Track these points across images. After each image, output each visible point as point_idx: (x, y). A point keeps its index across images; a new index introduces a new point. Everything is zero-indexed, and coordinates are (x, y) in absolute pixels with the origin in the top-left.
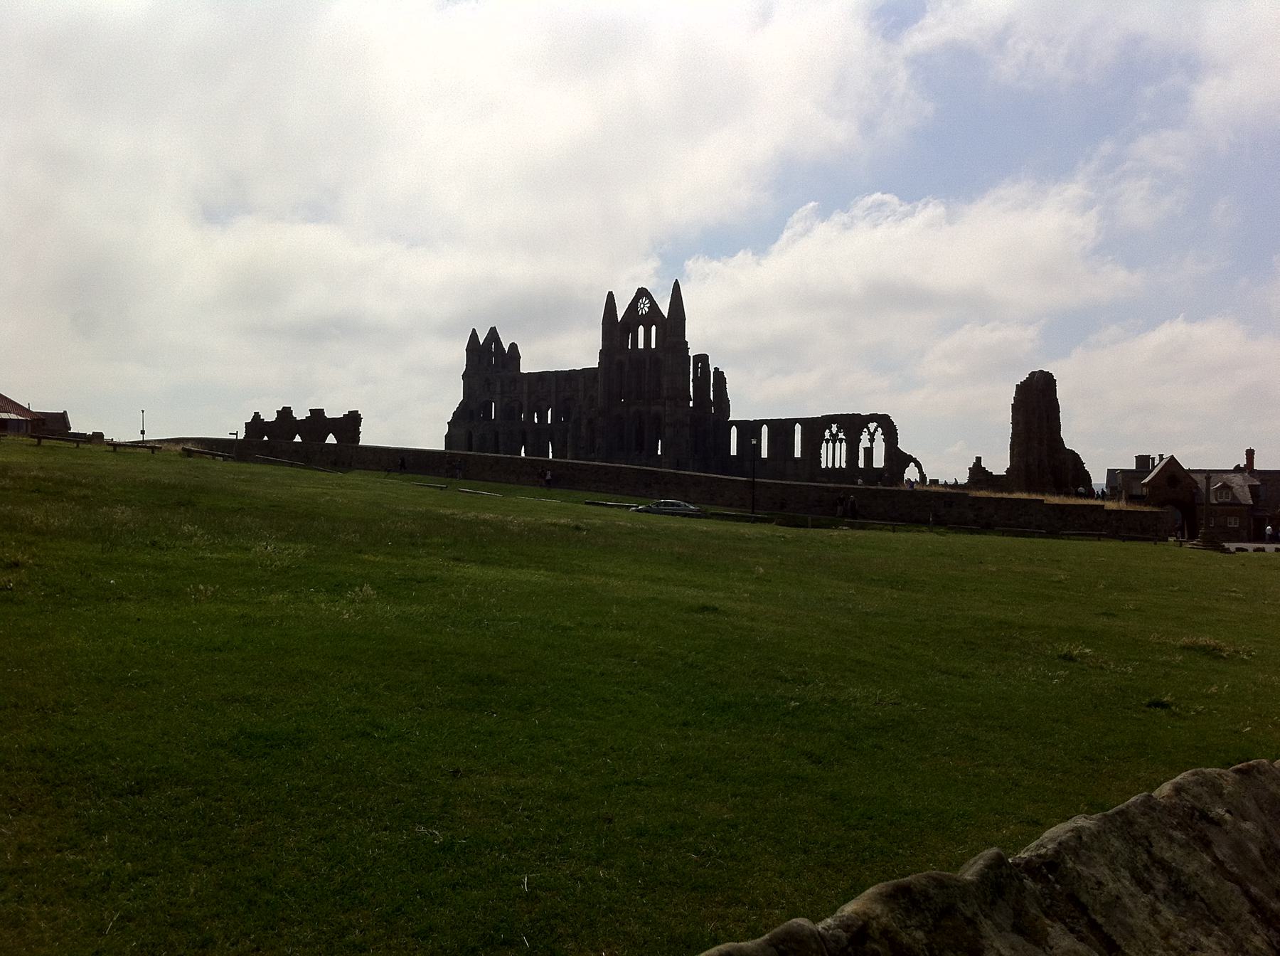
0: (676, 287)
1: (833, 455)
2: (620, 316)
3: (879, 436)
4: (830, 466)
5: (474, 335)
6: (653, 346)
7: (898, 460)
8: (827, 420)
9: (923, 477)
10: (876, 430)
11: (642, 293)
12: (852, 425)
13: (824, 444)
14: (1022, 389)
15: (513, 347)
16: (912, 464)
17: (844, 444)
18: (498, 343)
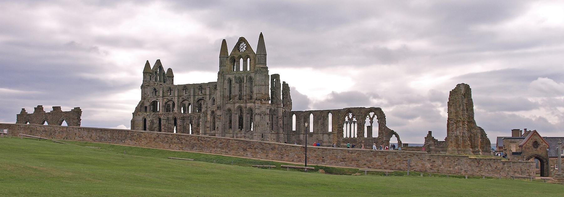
0: (261, 36)
1: (350, 131)
3: (375, 120)
4: (348, 136)
5: (148, 64)
6: (248, 70)
7: (386, 133)
8: (349, 110)
9: (400, 142)
10: (374, 116)
11: (242, 40)
12: (360, 114)
13: (345, 125)
15: (170, 70)
16: (394, 136)
17: (356, 124)
18: (161, 67)
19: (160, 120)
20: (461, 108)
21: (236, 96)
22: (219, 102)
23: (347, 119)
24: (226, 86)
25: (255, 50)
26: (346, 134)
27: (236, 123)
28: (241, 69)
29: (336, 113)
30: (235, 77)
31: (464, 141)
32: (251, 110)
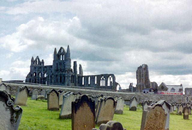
1: (102, 83)
2: (57, 52)
3: (112, 79)
5: (33, 58)
6: (64, 59)
8: (102, 75)
11: (61, 48)
12: (106, 76)
13: (101, 81)
14: (140, 68)
15: (43, 60)
18: (39, 59)
19: (36, 79)
20: (142, 74)
21: (59, 69)
22: (53, 72)
23: (101, 79)
24: (56, 65)
25: (66, 51)
26: (101, 85)
27: (59, 81)
28: (61, 59)
29: (98, 76)
30: (59, 62)
31: (143, 87)
32: (64, 75)
